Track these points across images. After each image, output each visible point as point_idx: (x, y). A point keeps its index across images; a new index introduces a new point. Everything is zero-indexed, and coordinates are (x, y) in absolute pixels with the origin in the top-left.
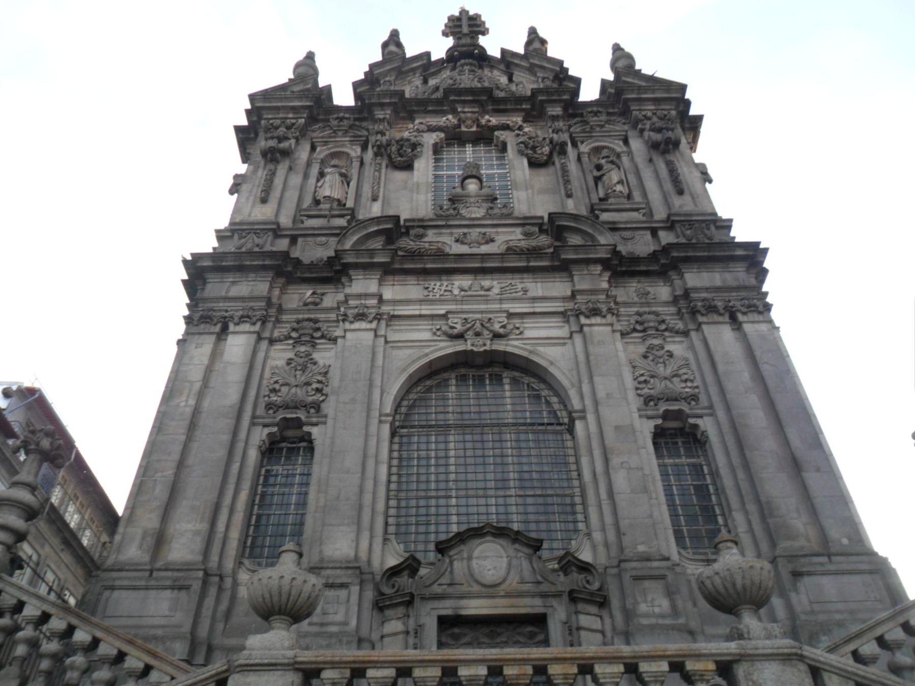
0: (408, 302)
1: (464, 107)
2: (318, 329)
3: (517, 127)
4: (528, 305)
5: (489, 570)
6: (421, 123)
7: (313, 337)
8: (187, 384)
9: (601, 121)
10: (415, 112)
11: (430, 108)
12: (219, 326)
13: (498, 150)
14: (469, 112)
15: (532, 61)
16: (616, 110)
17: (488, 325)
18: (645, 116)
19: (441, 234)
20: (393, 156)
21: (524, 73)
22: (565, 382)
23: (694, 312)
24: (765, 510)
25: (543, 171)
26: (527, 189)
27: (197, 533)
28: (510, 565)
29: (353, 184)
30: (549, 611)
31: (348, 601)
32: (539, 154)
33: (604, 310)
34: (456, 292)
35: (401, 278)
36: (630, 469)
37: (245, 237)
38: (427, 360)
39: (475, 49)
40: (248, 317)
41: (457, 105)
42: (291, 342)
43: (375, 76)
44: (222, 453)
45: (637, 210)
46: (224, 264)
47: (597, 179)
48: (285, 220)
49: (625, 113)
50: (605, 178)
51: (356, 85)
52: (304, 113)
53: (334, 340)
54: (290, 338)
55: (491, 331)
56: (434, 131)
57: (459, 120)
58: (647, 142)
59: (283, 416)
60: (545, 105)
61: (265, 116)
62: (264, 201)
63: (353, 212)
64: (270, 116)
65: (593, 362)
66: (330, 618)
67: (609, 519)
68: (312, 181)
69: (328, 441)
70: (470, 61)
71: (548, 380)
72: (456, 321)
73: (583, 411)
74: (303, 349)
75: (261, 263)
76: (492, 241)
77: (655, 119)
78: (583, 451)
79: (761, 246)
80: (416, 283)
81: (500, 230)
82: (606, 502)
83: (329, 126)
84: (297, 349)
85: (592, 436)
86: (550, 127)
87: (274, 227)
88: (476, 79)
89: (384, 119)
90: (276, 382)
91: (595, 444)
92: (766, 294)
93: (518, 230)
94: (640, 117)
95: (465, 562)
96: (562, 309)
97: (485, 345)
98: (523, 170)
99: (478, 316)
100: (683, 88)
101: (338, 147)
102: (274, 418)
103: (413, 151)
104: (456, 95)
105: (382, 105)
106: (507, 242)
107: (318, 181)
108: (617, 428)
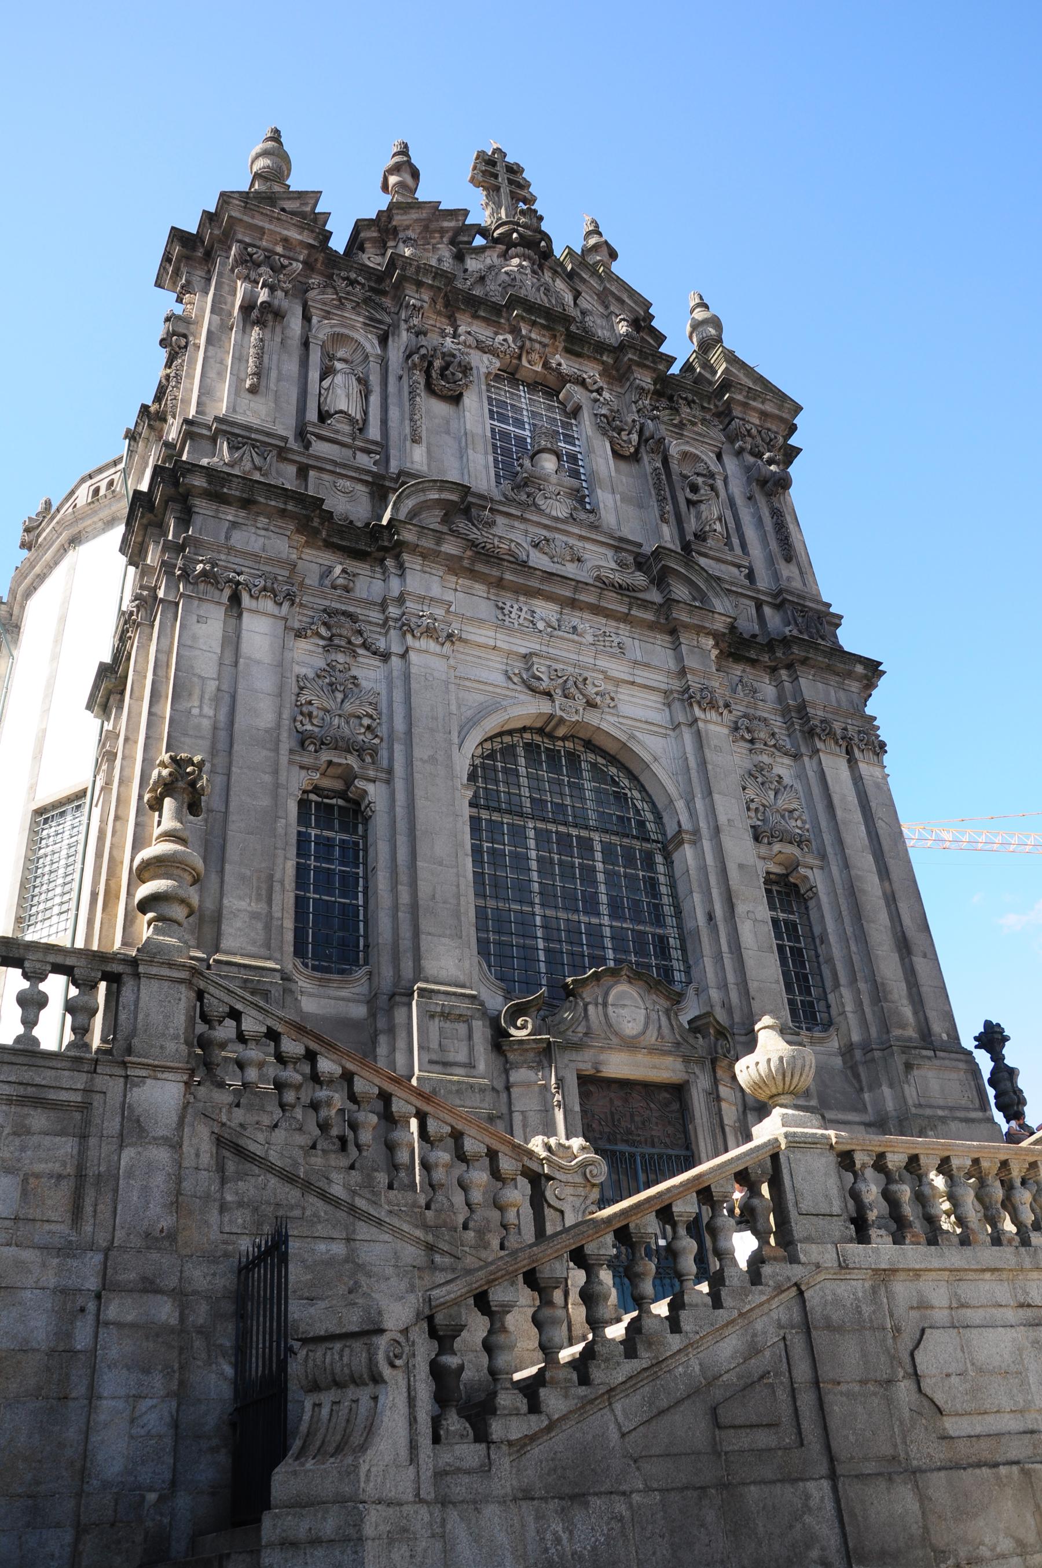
0: (481, 622)
1: (530, 331)
2: (360, 633)
3: (595, 387)
4: (627, 670)
5: (629, 1022)
6: (469, 333)
7: (349, 642)
8: (195, 679)
9: (694, 417)
10: (459, 309)
11: (482, 314)
12: (227, 592)
13: (565, 411)
14: (536, 341)
15: (608, 286)
16: (712, 407)
17: (581, 686)
18: (749, 431)
19: (513, 527)
20: (434, 375)
21: (591, 296)
22: (672, 789)
23: (810, 734)
24: (879, 993)
25: (623, 466)
26: (613, 493)
27: (255, 916)
28: (648, 1017)
29: (375, 399)
30: (692, 1078)
31: (470, 1037)
32: (624, 441)
33: (721, 703)
34: (541, 625)
35: (468, 582)
36: (755, 921)
37: (238, 448)
39: (542, 239)
40: (273, 591)
41: (522, 325)
42: (322, 643)
43: (394, 223)
44: (265, 802)
45: (739, 566)
46: (225, 490)
47: (690, 502)
49: (725, 415)
50: (703, 507)
51: (360, 226)
52: (300, 253)
53: (385, 657)
54: (318, 634)
55: (584, 695)
56: (486, 353)
57: (521, 348)
58: (748, 469)
59: (329, 758)
60: (634, 368)
61: (240, 237)
64: (247, 240)
65: (711, 774)
66: (451, 1057)
67: (731, 978)
68: (314, 375)
69: (400, 811)
70: (531, 253)
71: (642, 778)
72: (543, 669)
73: (696, 832)
74: (341, 658)
75: (282, 506)
76: (579, 560)
77: (759, 440)
79: (880, 668)
80: (485, 595)
81: (589, 546)
82: (729, 955)
83: (334, 288)
84: (333, 656)
85: (710, 869)
86: (635, 403)
87: (282, 444)
88: (542, 289)
89: (422, 307)
90: (310, 703)
92: (878, 728)
93: (610, 553)
94: (743, 430)
95: (600, 1007)
96: (664, 687)
97: (577, 712)
98: (607, 460)
99: (570, 669)
100: (797, 409)
101: (345, 327)
102: (316, 759)
103: (466, 376)
104: (524, 310)
105: (419, 284)
106: (599, 567)
107: (322, 380)
108: (741, 866)
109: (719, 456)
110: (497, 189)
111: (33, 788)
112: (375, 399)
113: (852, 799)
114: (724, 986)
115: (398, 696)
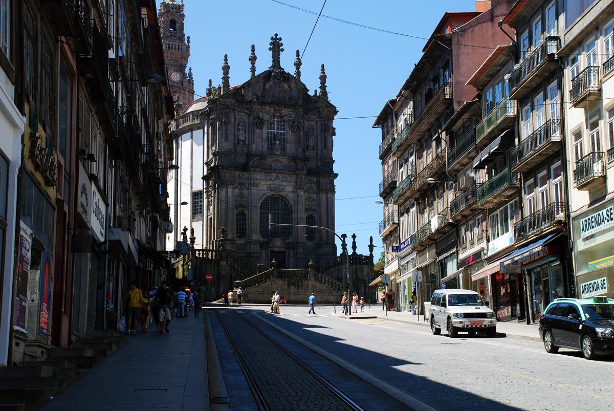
0: (263, 180)
29: (247, 134)
38: (265, 196)
47: (307, 139)
48: (232, 147)
53: (248, 189)
62: (227, 141)
63: (248, 146)
68: (236, 131)
74: (242, 191)
78: (294, 220)
91: (296, 220)
109: (317, 122)
110: (275, 50)
111: (192, 187)
112: (247, 134)
113: (325, 202)
114: (295, 236)
115: (250, 197)
